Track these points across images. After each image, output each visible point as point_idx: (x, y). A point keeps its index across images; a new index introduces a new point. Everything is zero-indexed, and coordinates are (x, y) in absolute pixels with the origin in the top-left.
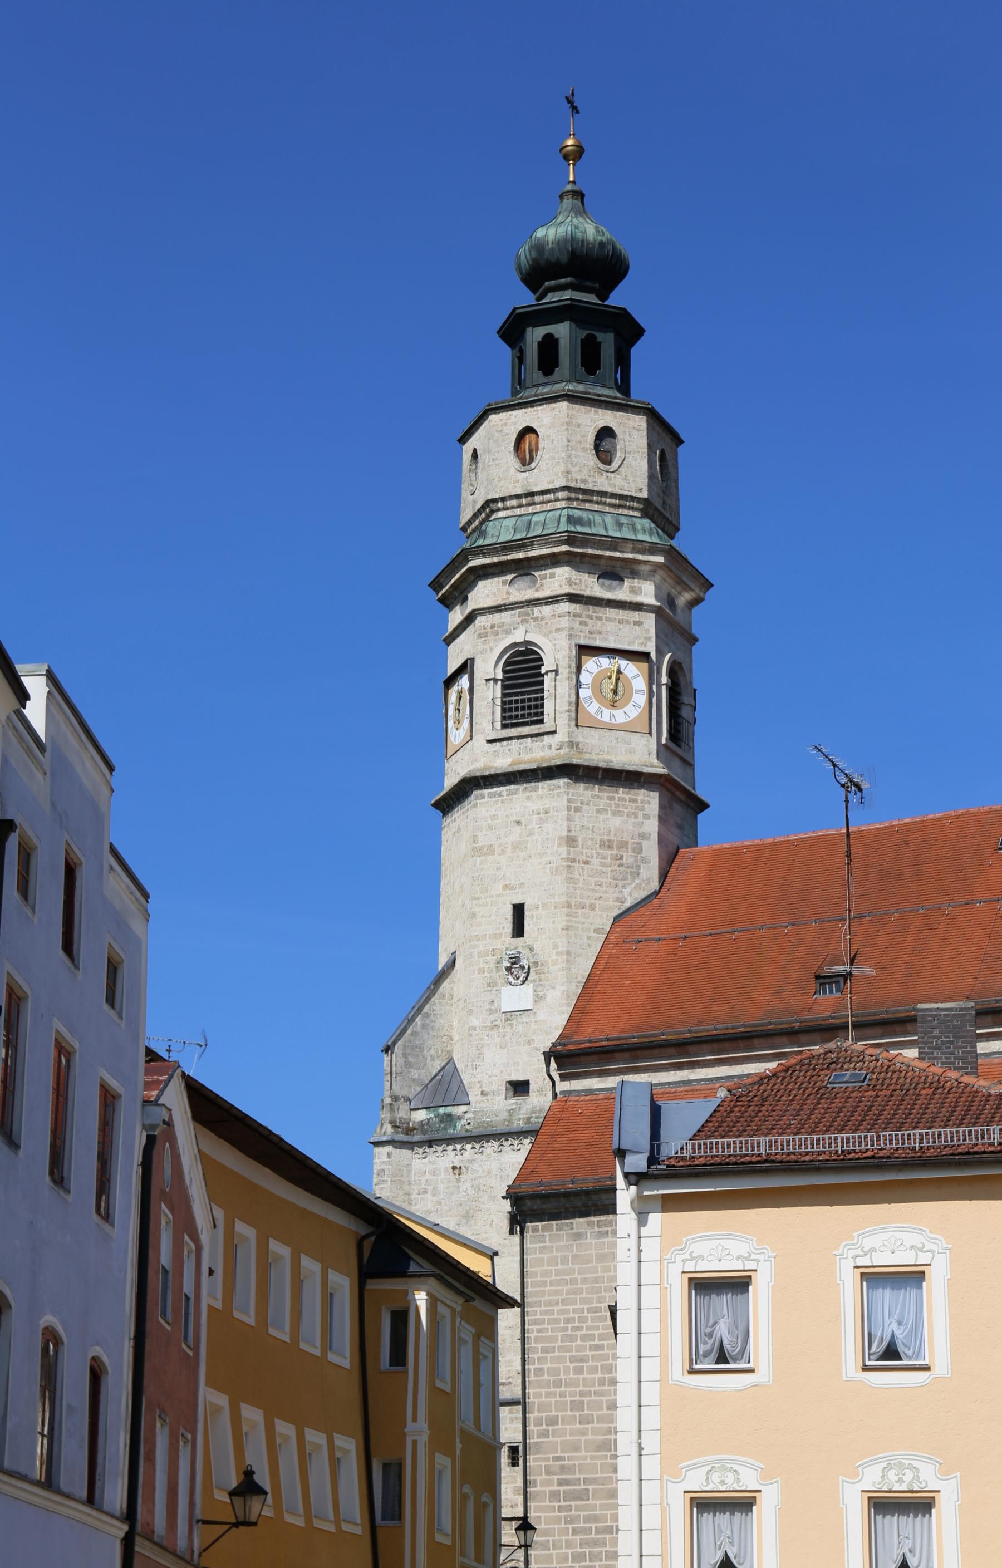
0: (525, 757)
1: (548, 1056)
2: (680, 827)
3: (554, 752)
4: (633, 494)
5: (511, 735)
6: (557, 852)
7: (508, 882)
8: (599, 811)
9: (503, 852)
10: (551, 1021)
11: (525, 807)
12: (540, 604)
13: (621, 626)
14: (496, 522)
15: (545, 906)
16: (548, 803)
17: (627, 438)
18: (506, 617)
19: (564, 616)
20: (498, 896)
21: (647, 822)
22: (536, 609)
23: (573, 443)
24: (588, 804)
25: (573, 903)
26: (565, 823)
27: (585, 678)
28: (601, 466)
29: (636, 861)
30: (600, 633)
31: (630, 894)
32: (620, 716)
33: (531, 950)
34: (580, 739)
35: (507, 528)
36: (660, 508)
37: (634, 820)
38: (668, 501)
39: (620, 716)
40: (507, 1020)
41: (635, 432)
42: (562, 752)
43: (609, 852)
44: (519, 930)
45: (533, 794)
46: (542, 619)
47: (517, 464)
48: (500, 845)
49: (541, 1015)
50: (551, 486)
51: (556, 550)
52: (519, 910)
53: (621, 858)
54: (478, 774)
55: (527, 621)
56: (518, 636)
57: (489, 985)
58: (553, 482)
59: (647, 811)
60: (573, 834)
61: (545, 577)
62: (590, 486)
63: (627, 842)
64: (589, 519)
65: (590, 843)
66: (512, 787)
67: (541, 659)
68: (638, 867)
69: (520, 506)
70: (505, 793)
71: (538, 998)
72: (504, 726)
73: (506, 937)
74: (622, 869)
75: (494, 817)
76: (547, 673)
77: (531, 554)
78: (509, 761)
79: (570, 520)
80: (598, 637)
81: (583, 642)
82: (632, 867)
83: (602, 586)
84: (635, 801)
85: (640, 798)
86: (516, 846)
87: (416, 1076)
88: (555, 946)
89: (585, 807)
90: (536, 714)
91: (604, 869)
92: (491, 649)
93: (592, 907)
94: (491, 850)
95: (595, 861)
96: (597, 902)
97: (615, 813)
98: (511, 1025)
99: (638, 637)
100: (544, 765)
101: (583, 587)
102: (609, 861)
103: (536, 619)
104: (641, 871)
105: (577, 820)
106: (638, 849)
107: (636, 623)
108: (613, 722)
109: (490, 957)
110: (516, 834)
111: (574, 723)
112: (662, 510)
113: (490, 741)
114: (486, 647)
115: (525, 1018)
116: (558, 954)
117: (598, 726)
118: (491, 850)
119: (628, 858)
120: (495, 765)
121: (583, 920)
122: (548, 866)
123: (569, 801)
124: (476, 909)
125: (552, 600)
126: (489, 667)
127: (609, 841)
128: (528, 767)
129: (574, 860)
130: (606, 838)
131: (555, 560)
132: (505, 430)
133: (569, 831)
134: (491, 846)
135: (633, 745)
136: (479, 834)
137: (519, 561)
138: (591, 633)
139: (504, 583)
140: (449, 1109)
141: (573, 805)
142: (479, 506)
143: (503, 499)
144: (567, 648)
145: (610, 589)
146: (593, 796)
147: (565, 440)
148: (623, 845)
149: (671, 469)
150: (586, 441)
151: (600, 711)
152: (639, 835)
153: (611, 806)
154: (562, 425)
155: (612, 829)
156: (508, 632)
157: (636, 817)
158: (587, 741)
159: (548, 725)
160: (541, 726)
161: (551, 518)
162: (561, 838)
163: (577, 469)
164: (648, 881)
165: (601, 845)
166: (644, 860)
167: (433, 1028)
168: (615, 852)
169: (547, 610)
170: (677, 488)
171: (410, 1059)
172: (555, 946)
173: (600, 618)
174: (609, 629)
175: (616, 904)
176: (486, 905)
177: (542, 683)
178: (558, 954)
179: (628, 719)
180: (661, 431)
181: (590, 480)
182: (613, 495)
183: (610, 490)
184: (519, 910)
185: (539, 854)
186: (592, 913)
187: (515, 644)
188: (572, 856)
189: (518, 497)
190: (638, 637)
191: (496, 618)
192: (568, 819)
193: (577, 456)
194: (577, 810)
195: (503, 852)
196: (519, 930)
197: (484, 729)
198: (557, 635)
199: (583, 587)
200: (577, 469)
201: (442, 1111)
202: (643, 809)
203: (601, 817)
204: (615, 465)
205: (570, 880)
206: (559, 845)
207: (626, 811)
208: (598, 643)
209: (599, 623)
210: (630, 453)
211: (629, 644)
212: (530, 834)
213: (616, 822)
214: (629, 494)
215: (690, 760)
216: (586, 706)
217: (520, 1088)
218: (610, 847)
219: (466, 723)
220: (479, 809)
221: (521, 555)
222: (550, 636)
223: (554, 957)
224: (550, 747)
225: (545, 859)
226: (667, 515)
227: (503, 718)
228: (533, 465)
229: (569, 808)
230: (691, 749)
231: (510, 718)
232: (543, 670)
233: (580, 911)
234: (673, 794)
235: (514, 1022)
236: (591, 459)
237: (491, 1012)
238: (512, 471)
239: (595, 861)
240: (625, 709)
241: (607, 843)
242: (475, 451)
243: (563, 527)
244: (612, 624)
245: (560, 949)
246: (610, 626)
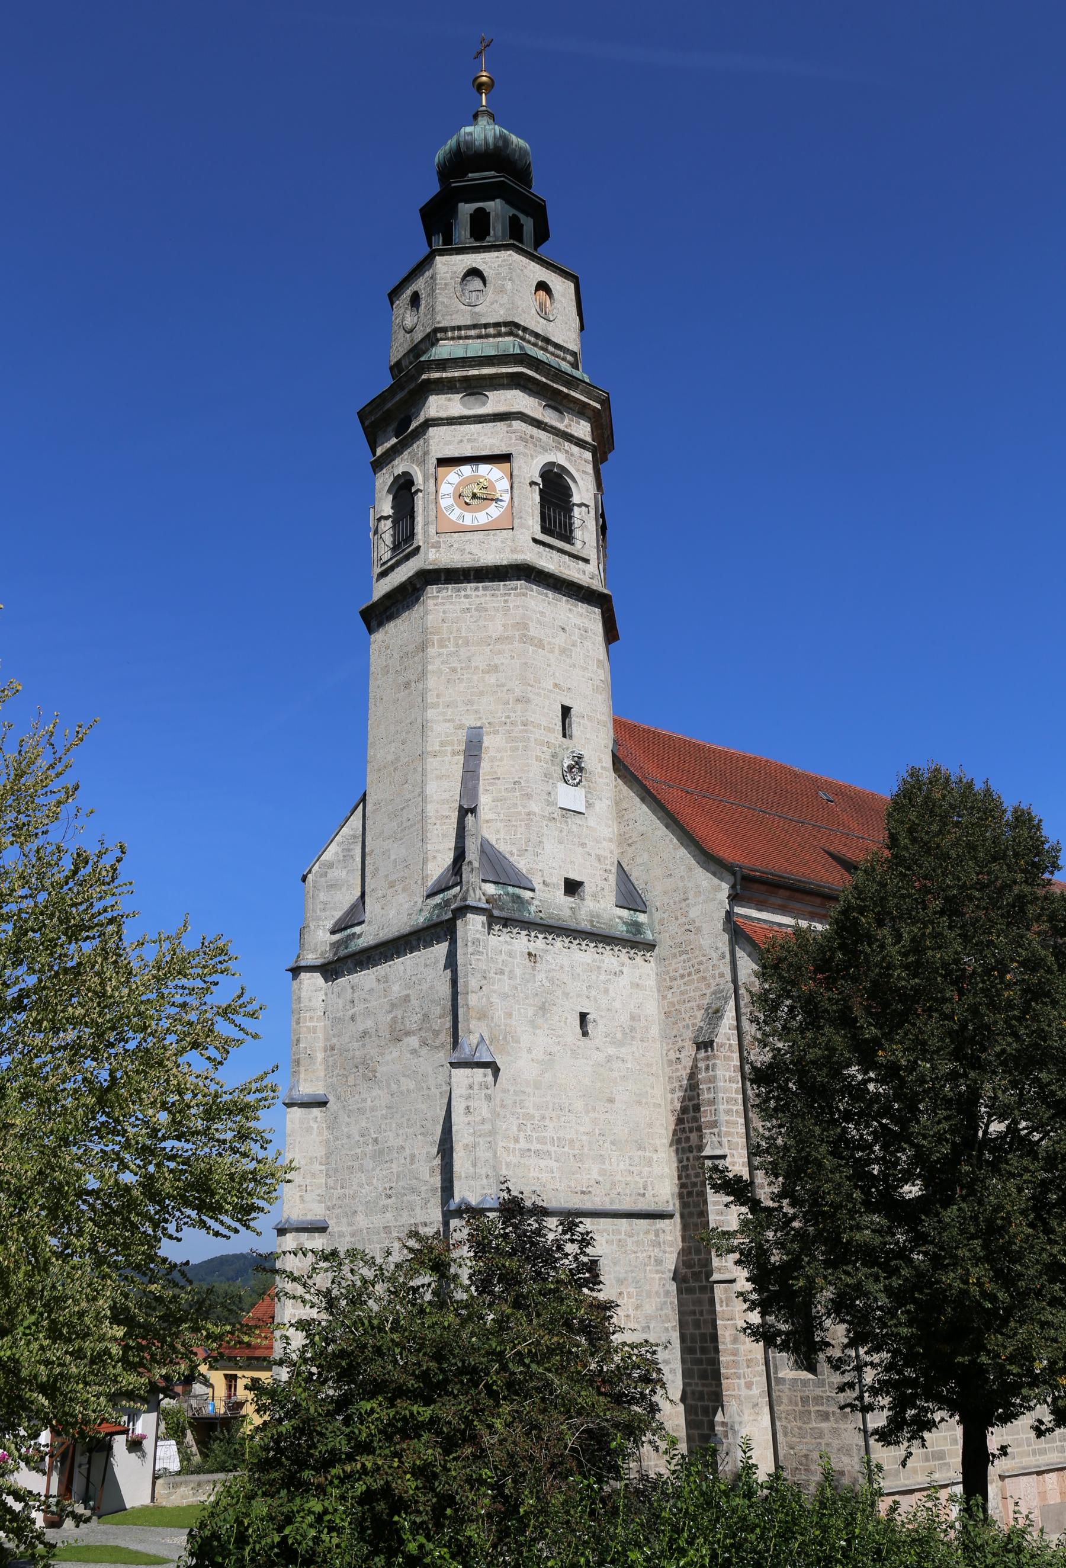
12: (571, 442)
15: (590, 719)
18: (542, 435)
22: (566, 444)
40: (563, 816)
49: (592, 822)
56: (561, 459)
69: (535, 345)
71: (589, 805)
86: (563, 651)
88: (600, 761)
94: (540, 645)
98: (566, 822)
109: (545, 749)
110: (561, 639)
113: (535, 541)
139: (540, 404)
140: (517, 891)
143: (525, 329)
169: (575, 449)
172: (600, 761)
176: (539, 694)
189: (537, 335)
191: (536, 432)
195: (552, 651)
201: (510, 889)
217: (572, 887)
221: (565, 390)
237: (550, 803)
238: (533, 311)
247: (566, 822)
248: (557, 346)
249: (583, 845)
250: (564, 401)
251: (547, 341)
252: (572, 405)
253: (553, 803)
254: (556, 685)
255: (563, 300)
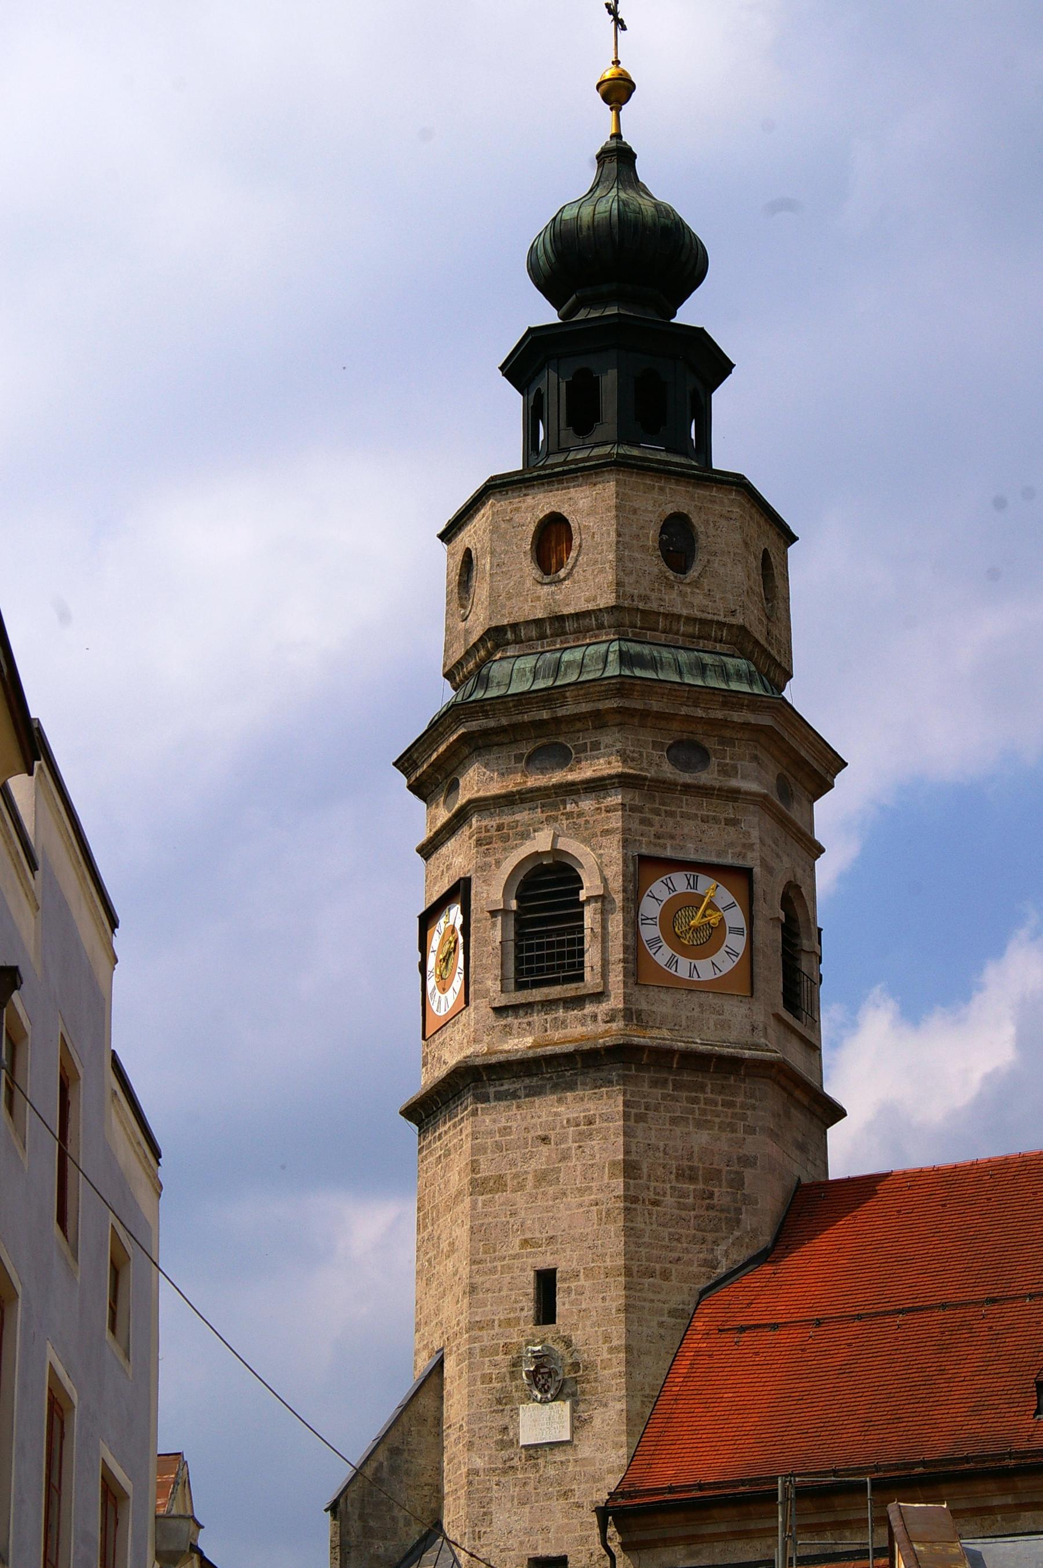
0: (557, 1035)
1: (603, 1513)
2: (802, 1148)
3: (602, 1027)
4: (721, 618)
5: (531, 999)
6: (608, 1186)
7: (528, 1235)
8: (674, 1121)
9: (521, 1187)
10: (604, 1459)
11: (556, 1114)
12: (577, 792)
13: (705, 826)
14: (504, 663)
15: (589, 1273)
16: (592, 1107)
17: (712, 531)
19: (615, 810)
20: (515, 1257)
21: (750, 1138)
23: (627, 539)
24: (656, 1110)
25: (635, 1269)
26: (621, 1140)
27: (650, 908)
28: (670, 574)
29: (735, 1201)
30: (672, 837)
31: (726, 1254)
32: (706, 970)
33: (568, 1343)
34: (644, 1006)
35: (522, 672)
36: (763, 642)
37: (730, 1135)
38: (775, 632)
39: (706, 970)
40: (530, 1458)
41: (723, 522)
42: (614, 1025)
43: (692, 1187)
44: (546, 1313)
45: (569, 1095)
46: (580, 815)
47: (537, 573)
48: (516, 1176)
49: (585, 1450)
50: (591, 606)
51: (603, 705)
52: (546, 1283)
53: (711, 1195)
54: (478, 1061)
55: (555, 819)
56: (542, 842)
57: (499, 1401)
58: (595, 599)
59: (750, 1122)
60: (633, 1157)
61: (583, 749)
62: (654, 606)
63: (720, 1171)
64: (653, 658)
65: (660, 1171)
66: (534, 1081)
67: (578, 879)
68: (738, 1211)
70: (522, 1093)
71: (578, 1423)
72: (520, 986)
73: (526, 1323)
74: (712, 1213)
75: (505, 1131)
76: (589, 899)
77: (561, 712)
78: (529, 1040)
79: (625, 659)
80: (669, 843)
81: (644, 851)
82: (728, 1211)
83: (675, 762)
84: (731, 1104)
85: (739, 1100)
86: (542, 1178)
87: (382, 1551)
88: (607, 1339)
89: (651, 1114)
90: (572, 966)
91: (684, 1213)
92: (498, 863)
93: (665, 1275)
94: (499, 1183)
95: (669, 1200)
96: (673, 1267)
97: (700, 1125)
99: (731, 845)
100: (587, 1046)
101: (645, 765)
102: (691, 1200)
103: (569, 815)
104: (743, 1217)
105: (640, 1133)
106: (737, 1182)
107: (729, 822)
108: (695, 978)
109: (500, 1357)
110: (542, 1157)
111: (631, 981)
112: (766, 646)
113: (499, 1011)
114: (490, 859)
115: (559, 1456)
116: (611, 1350)
117: (673, 984)
118: (499, 1183)
119: (721, 1194)
120: (506, 1047)
121: (651, 1296)
122: (595, 1208)
123: (626, 1104)
124: (478, 1279)
125: (596, 786)
126: (492, 893)
127: (691, 1168)
128: (558, 1049)
129: (635, 1200)
130: (686, 1163)
131: (598, 720)
132: (517, 518)
133: (627, 1152)
134: (501, 1177)
135: (727, 1016)
136: (482, 1158)
137: (543, 722)
138: (657, 836)
139: (518, 758)
141: (633, 1111)
142: (474, 638)
143: (514, 626)
144: (620, 862)
145: (686, 767)
146: (664, 1097)
147: (613, 534)
148: (712, 1176)
149: (778, 582)
150: (647, 536)
151: (672, 961)
152: (739, 1159)
153: (693, 1112)
154: (608, 510)
155: (696, 1149)
156: (525, 836)
157: (734, 1131)
158: (654, 1008)
159: (591, 979)
160: (581, 984)
161: (593, 659)
162: (613, 1164)
163: (632, 579)
164: (754, 1233)
165: (678, 1176)
166: (747, 1200)
167: (408, 1473)
168: (700, 1186)
170: (788, 610)
171: (372, 1524)
172: (607, 1339)
173: (671, 814)
174: (686, 831)
175: (703, 1269)
176: (493, 1271)
177: (581, 916)
178: (611, 1350)
179: (719, 974)
180: (762, 522)
181: (654, 595)
182: (690, 620)
183: (684, 612)
184: (546, 1283)
185: (579, 1190)
186: (665, 1284)
187: (537, 854)
188: (632, 1193)
189: (538, 622)
190: (731, 845)
192: (625, 1134)
193: (632, 560)
194: (640, 1118)
195: (521, 1187)
196: (546, 1313)
197: (488, 990)
198: (604, 841)
199: (645, 765)
200: (632, 579)
202: (744, 1117)
203: (678, 1130)
204: (693, 573)
205: (630, 1232)
206: (612, 1176)
207: (717, 1120)
208: (669, 853)
209: (670, 821)
210: (715, 554)
211: (719, 854)
212: (565, 1157)
213: (702, 1138)
214: (716, 618)
215: (813, 1040)
216: (651, 952)
218: (692, 1179)
219: (458, 982)
220: (480, 1118)
221: (545, 715)
222: (593, 841)
223: (606, 1355)
224: (594, 1017)
225: (587, 1198)
226: (774, 653)
227: (519, 972)
228: (562, 573)
229: (626, 1116)
230: (815, 1024)
231: (530, 972)
232: (583, 895)
233: (647, 1281)
234: (790, 1094)
235: (541, 1461)
236: (655, 565)
237: (503, 1445)
238: (529, 583)
239: (669, 1200)
240: (713, 958)
241: (687, 1172)
242: (468, 552)
243: (613, 670)
244: (692, 822)
245: (615, 1343)
246: (689, 827)
247: (536, 1465)
248: (578, 616)
249: (566, 1495)
250: (564, 728)
251: (561, 619)
252: (579, 725)
253: (512, 1443)
254: (525, 1243)
255: (590, 522)
